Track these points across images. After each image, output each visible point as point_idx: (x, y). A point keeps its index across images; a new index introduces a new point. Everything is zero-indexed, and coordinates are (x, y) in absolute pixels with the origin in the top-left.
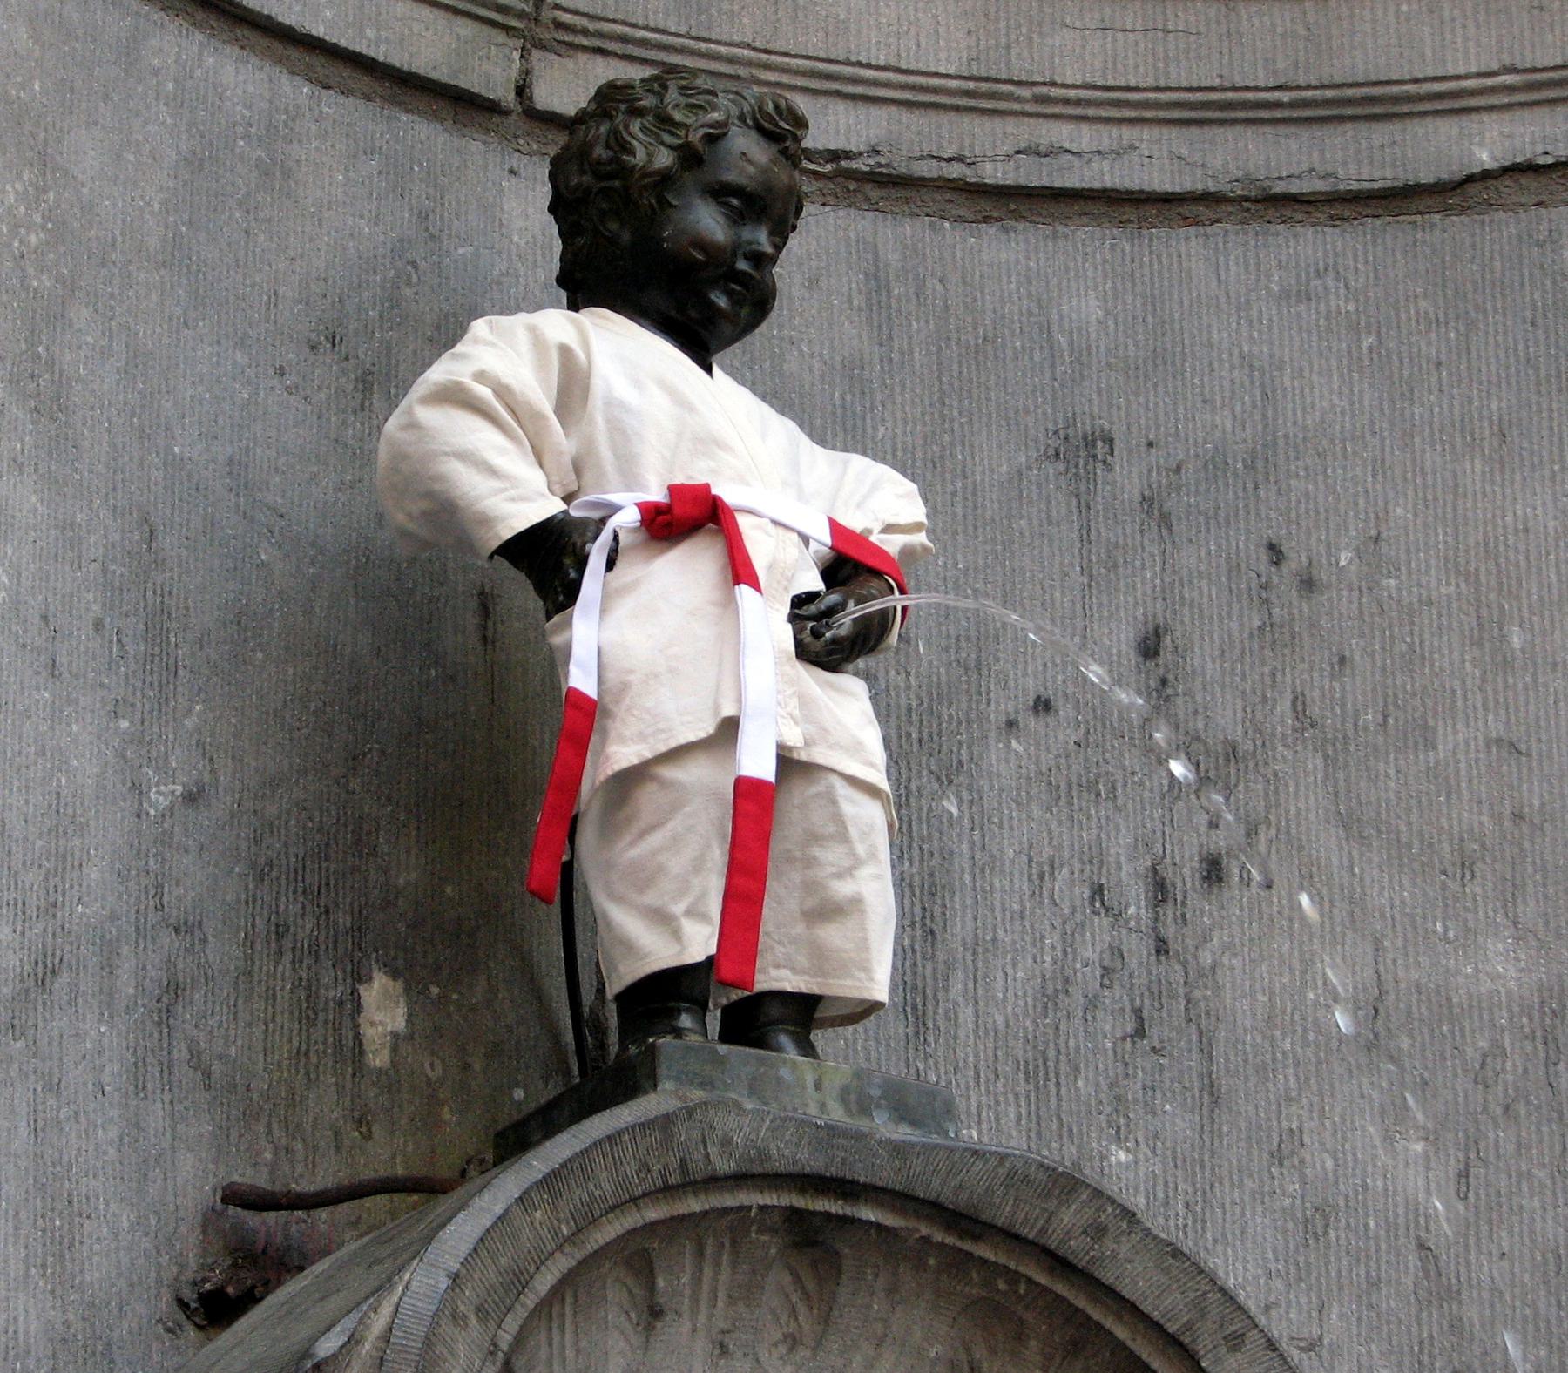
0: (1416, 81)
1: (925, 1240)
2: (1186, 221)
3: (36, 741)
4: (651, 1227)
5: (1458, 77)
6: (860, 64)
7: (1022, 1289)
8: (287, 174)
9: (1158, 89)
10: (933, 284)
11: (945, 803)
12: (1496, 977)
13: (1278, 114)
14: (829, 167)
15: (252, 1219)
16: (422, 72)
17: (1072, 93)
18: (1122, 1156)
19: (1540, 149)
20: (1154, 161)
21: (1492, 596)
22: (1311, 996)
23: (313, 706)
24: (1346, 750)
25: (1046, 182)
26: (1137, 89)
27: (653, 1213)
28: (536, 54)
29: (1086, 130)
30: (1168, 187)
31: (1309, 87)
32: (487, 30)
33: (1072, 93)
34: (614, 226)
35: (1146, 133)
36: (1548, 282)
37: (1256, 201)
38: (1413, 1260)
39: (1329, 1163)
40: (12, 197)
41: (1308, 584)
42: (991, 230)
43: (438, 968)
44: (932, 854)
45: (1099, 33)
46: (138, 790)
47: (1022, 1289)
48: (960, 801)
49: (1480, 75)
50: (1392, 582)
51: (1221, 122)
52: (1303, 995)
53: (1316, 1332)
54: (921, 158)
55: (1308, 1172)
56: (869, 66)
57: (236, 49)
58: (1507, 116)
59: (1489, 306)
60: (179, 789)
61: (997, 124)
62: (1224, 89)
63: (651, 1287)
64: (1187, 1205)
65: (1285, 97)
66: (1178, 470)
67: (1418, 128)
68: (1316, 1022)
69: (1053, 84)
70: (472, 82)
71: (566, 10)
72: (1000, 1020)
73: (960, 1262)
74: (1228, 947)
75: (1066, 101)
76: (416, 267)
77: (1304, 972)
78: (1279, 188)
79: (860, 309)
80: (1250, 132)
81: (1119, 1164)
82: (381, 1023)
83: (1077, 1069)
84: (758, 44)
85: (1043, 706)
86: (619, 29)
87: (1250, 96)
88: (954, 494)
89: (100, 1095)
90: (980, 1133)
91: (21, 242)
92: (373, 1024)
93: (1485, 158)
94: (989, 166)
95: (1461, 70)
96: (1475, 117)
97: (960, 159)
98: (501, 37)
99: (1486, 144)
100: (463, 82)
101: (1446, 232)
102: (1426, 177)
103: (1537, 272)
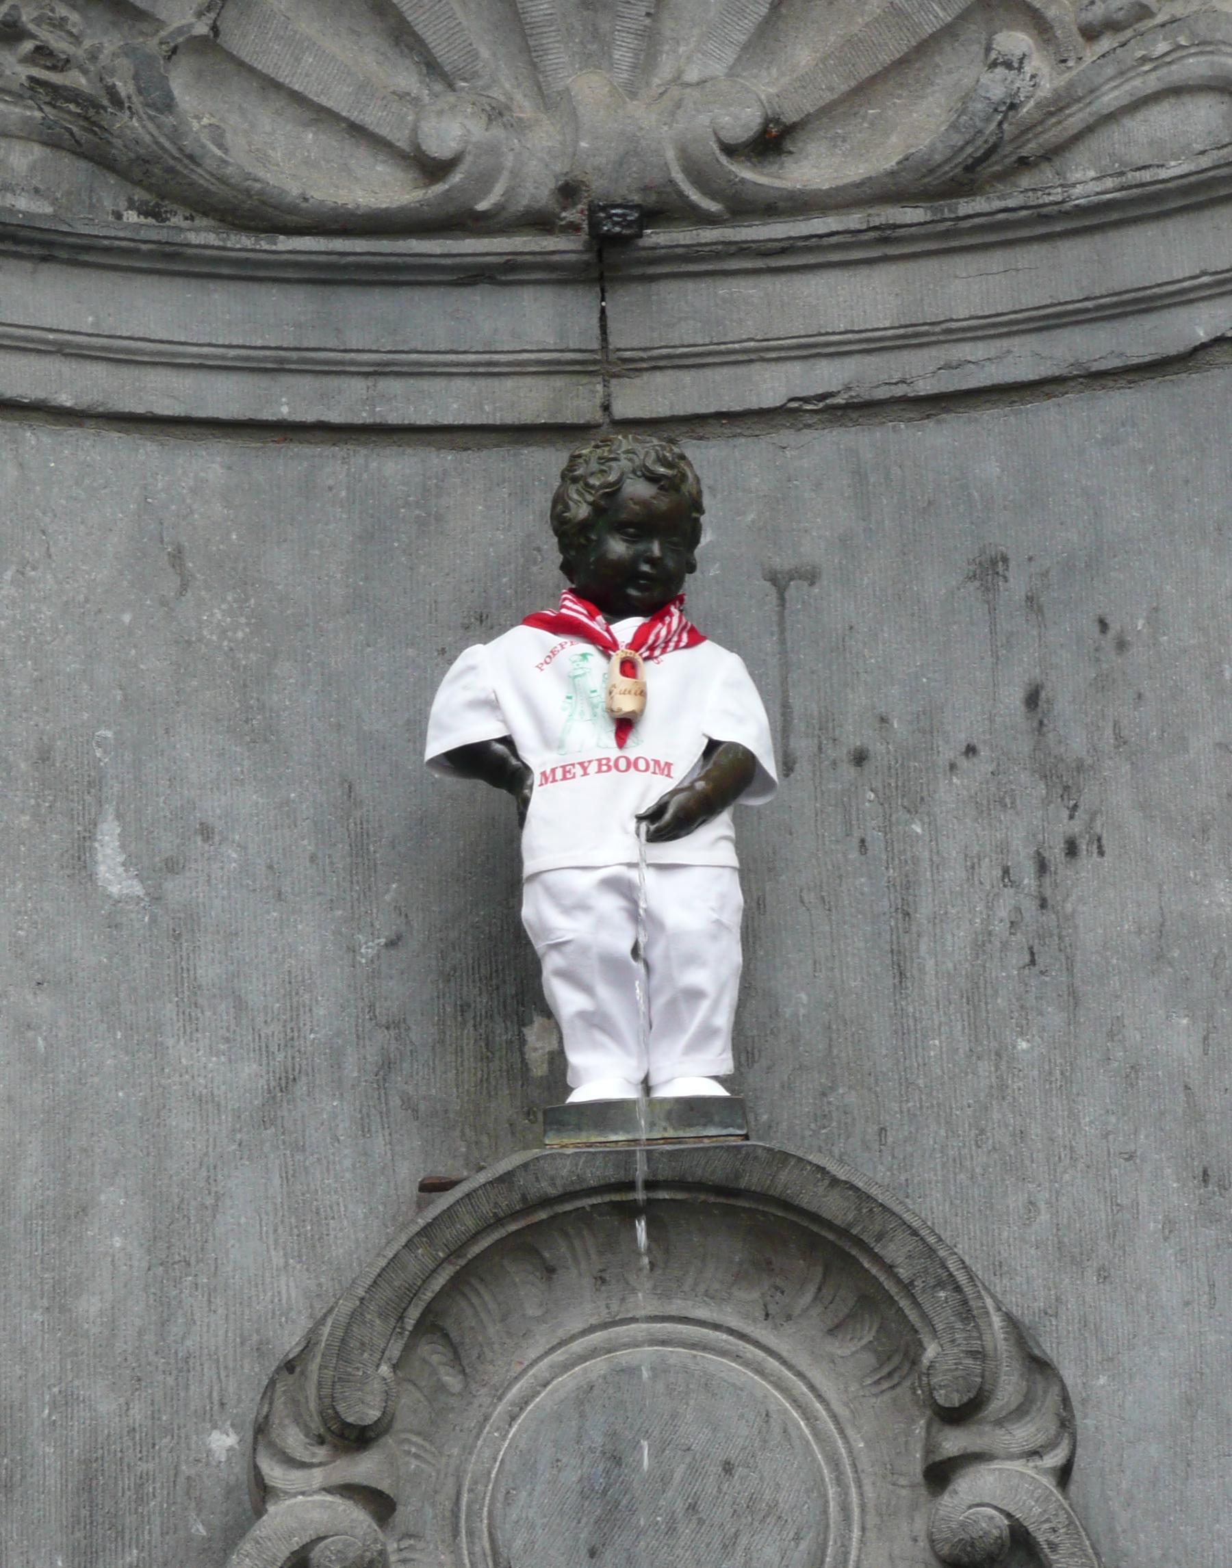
2: (1049, 396)
3: (269, 945)
5: (1179, 281)
6: (827, 334)
8: (439, 518)
10: (895, 470)
11: (913, 826)
12: (1220, 905)
14: (821, 405)
16: (528, 422)
20: (1022, 360)
23: (479, 861)
27: (513, 1227)
28: (614, 381)
29: (980, 345)
30: (1032, 377)
32: (575, 379)
33: (965, 324)
39: (1138, 1037)
40: (219, 616)
41: (1121, 645)
42: (930, 424)
44: (906, 862)
45: (978, 279)
46: (353, 950)
48: (923, 824)
50: (1166, 638)
52: (1122, 926)
53: (1132, 1147)
54: (877, 387)
56: (834, 333)
57: (395, 448)
58: (1212, 303)
60: (383, 941)
61: (925, 353)
64: (1062, 1073)
65: (1089, 304)
72: (950, 965)
73: (730, 1211)
74: (1081, 899)
75: (964, 330)
76: (539, 550)
77: (1122, 911)
78: (1095, 367)
79: (849, 498)
80: (1077, 329)
81: (1023, 1051)
82: (542, 1048)
83: (996, 991)
84: (758, 337)
85: (971, 750)
86: (664, 351)
87: (1070, 307)
88: (913, 615)
89: (336, 1144)
90: (941, 1042)
91: (230, 641)
92: (535, 1049)
93: (1202, 334)
94: (921, 383)
95: (1181, 277)
96: (1196, 305)
97: (903, 381)
98: (585, 380)
100: (560, 419)
102: (1172, 351)
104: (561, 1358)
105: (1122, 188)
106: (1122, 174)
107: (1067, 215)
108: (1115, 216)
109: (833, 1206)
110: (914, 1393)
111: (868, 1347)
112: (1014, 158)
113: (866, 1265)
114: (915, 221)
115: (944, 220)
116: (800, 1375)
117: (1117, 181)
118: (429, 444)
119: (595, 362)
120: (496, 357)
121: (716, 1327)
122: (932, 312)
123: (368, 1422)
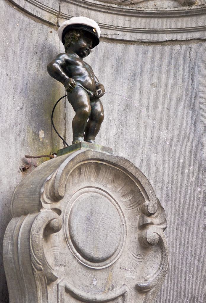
0: (159, 29)
1: (110, 166)
4: (82, 164)
7: (120, 172)
9: (129, 28)
13: (143, 32)
15: (28, 159)
17: (120, 28)
18: (122, 154)
19: (173, 38)
20: (129, 36)
21: (166, 91)
22: (144, 136)
24: (149, 108)
25: (116, 38)
26: (127, 28)
27: (82, 163)
28: (59, 18)
31: (147, 29)
33: (120, 28)
34: (73, 42)
35: (128, 33)
36: (173, 54)
37: (140, 42)
38: (155, 167)
43: (47, 129)
47: (120, 172)
49: (167, 29)
50: (154, 89)
51: (136, 32)
55: (143, 157)
59: (166, 56)
60: (20, 107)
62: (137, 28)
63: (80, 171)
65: (144, 30)
66: (130, 74)
67: (159, 35)
68: (144, 140)
69: (117, 26)
70: (51, 21)
71: (63, 13)
72: (109, 138)
74: (135, 130)
75: (119, 29)
77: (143, 134)
78: (143, 41)
86: (69, 16)
87: (140, 29)
93: (167, 39)
98: (55, 16)
99: (167, 37)
101: (161, 47)
102: (160, 41)
103: (172, 53)
104: (81, 192)
105: (157, 11)
106: (157, 8)
107: (143, 13)
108: (152, 16)
109: (133, 171)
110: (137, 210)
111: (130, 200)
112: (130, 2)
113: (136, 184)
114: (116, 7)
115: (121, 8)
116: (117, 203)
117: (156, 9)
118: (30, 18)
119: (58, 14)
120: (44, 6)
121: (105, 191)
122: (114, 24)
123: (62, 196)
